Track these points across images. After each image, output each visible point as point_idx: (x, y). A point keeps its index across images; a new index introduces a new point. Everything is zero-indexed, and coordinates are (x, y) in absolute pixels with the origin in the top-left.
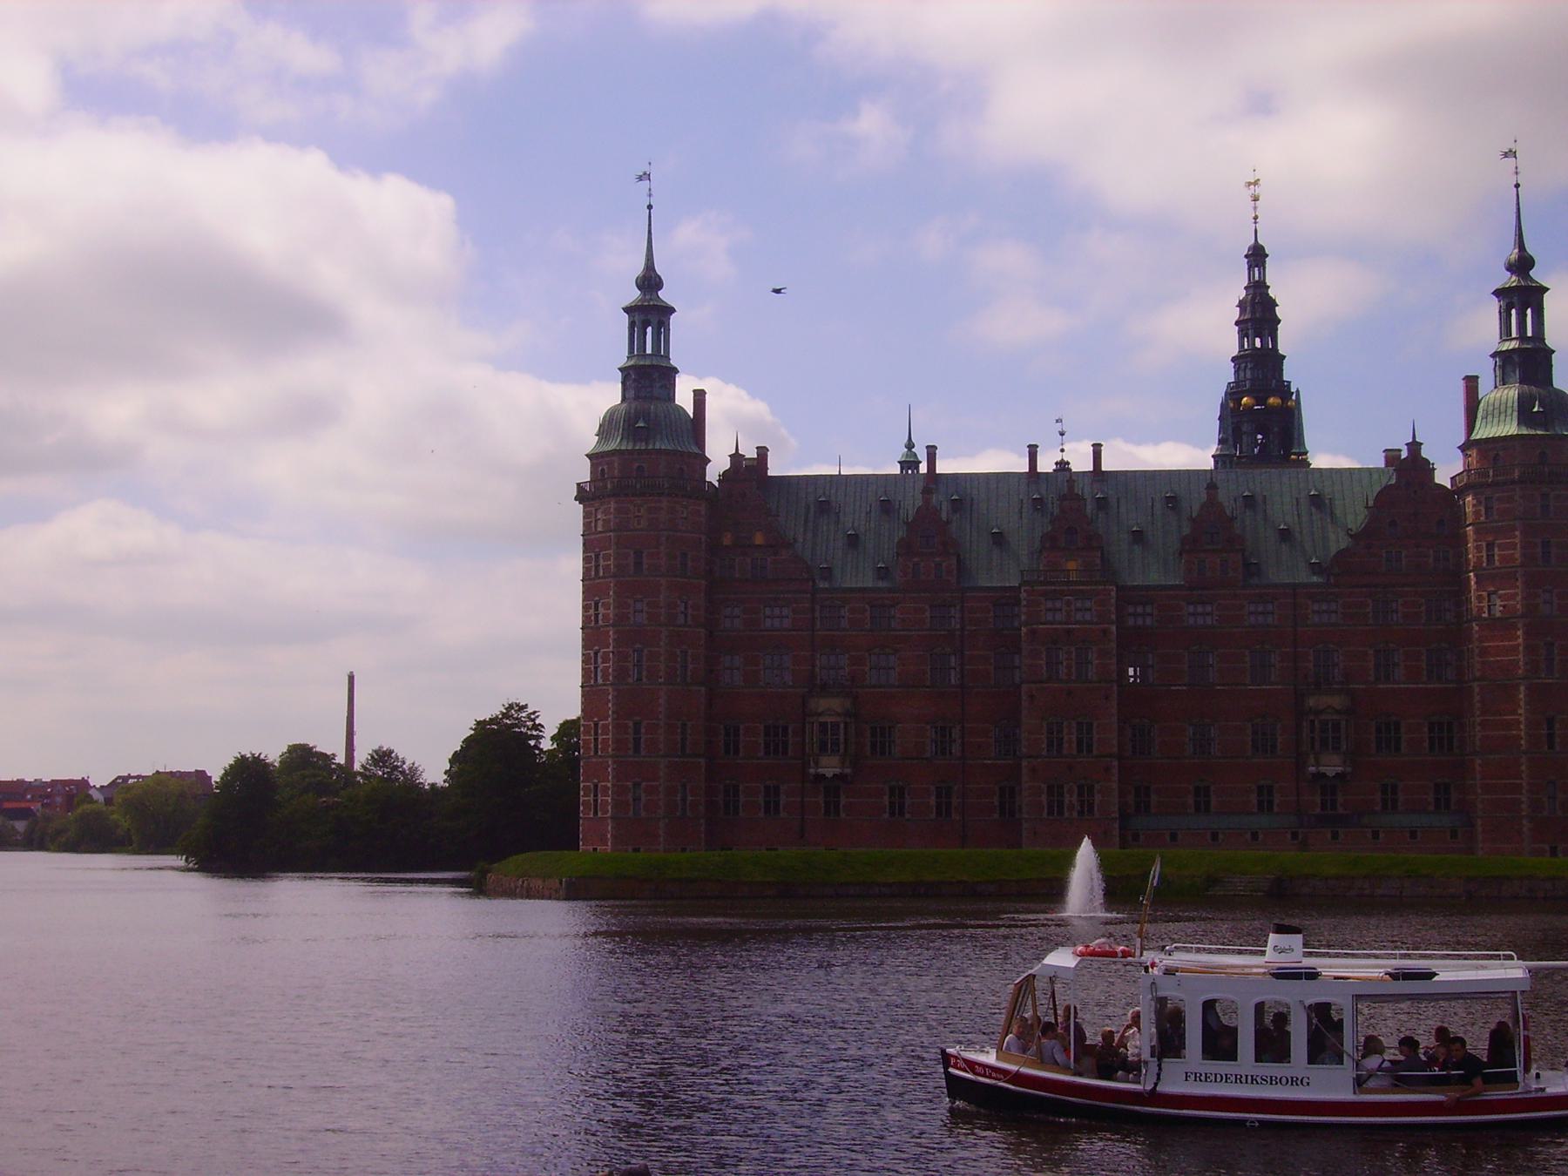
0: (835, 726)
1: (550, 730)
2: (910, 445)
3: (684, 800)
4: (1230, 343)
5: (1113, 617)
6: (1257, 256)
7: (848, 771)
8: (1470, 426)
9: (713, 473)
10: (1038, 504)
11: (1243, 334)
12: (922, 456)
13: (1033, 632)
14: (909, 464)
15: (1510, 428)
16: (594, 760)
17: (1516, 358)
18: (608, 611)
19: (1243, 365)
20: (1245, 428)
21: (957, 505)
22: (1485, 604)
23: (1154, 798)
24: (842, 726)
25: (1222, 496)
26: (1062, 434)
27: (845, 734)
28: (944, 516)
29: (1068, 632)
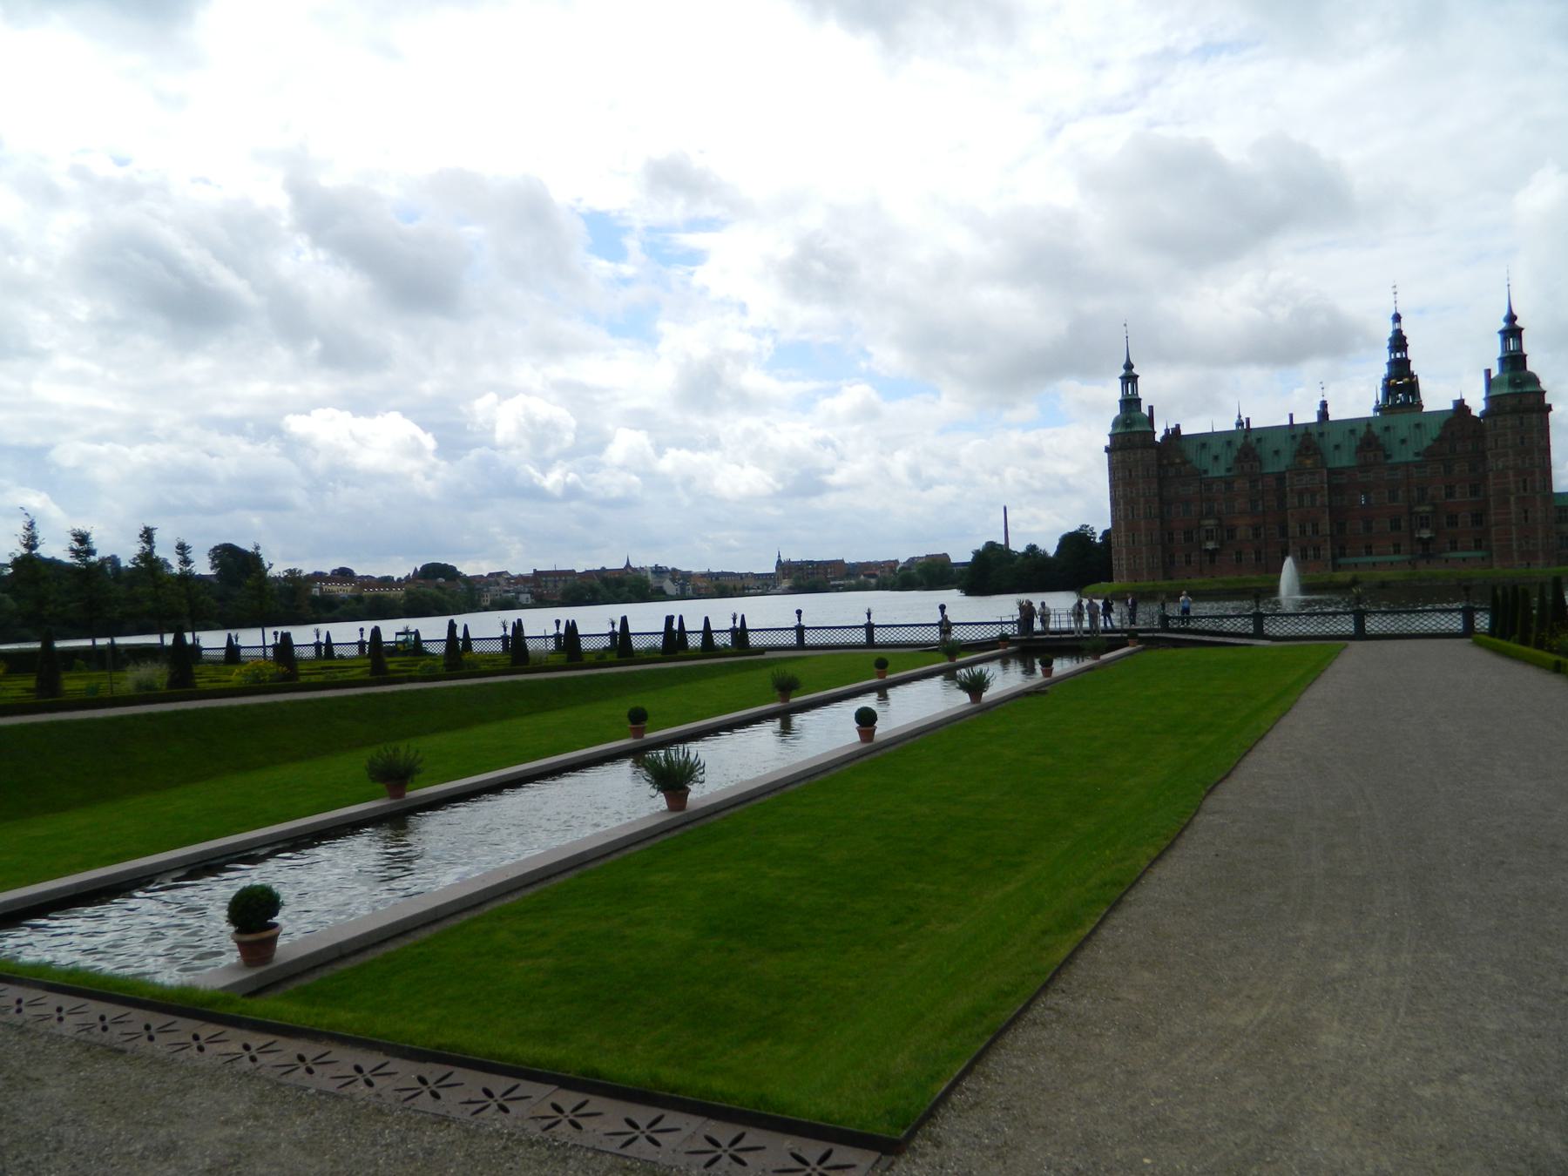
0: (1212, 531)
1: (1099, 534)
2: (1240, 416)
3: (1153, 562)
7: (1218, 547)
10: (1294, 437)
11: (1391, 352)
12: (1245, 421)
13: (1292, 490)
14: (1240, 424)
15: (1505, 390)
17: (1508, 360)
21: (1259, 440)
26: (1323, 388)
29: (1307, 489)
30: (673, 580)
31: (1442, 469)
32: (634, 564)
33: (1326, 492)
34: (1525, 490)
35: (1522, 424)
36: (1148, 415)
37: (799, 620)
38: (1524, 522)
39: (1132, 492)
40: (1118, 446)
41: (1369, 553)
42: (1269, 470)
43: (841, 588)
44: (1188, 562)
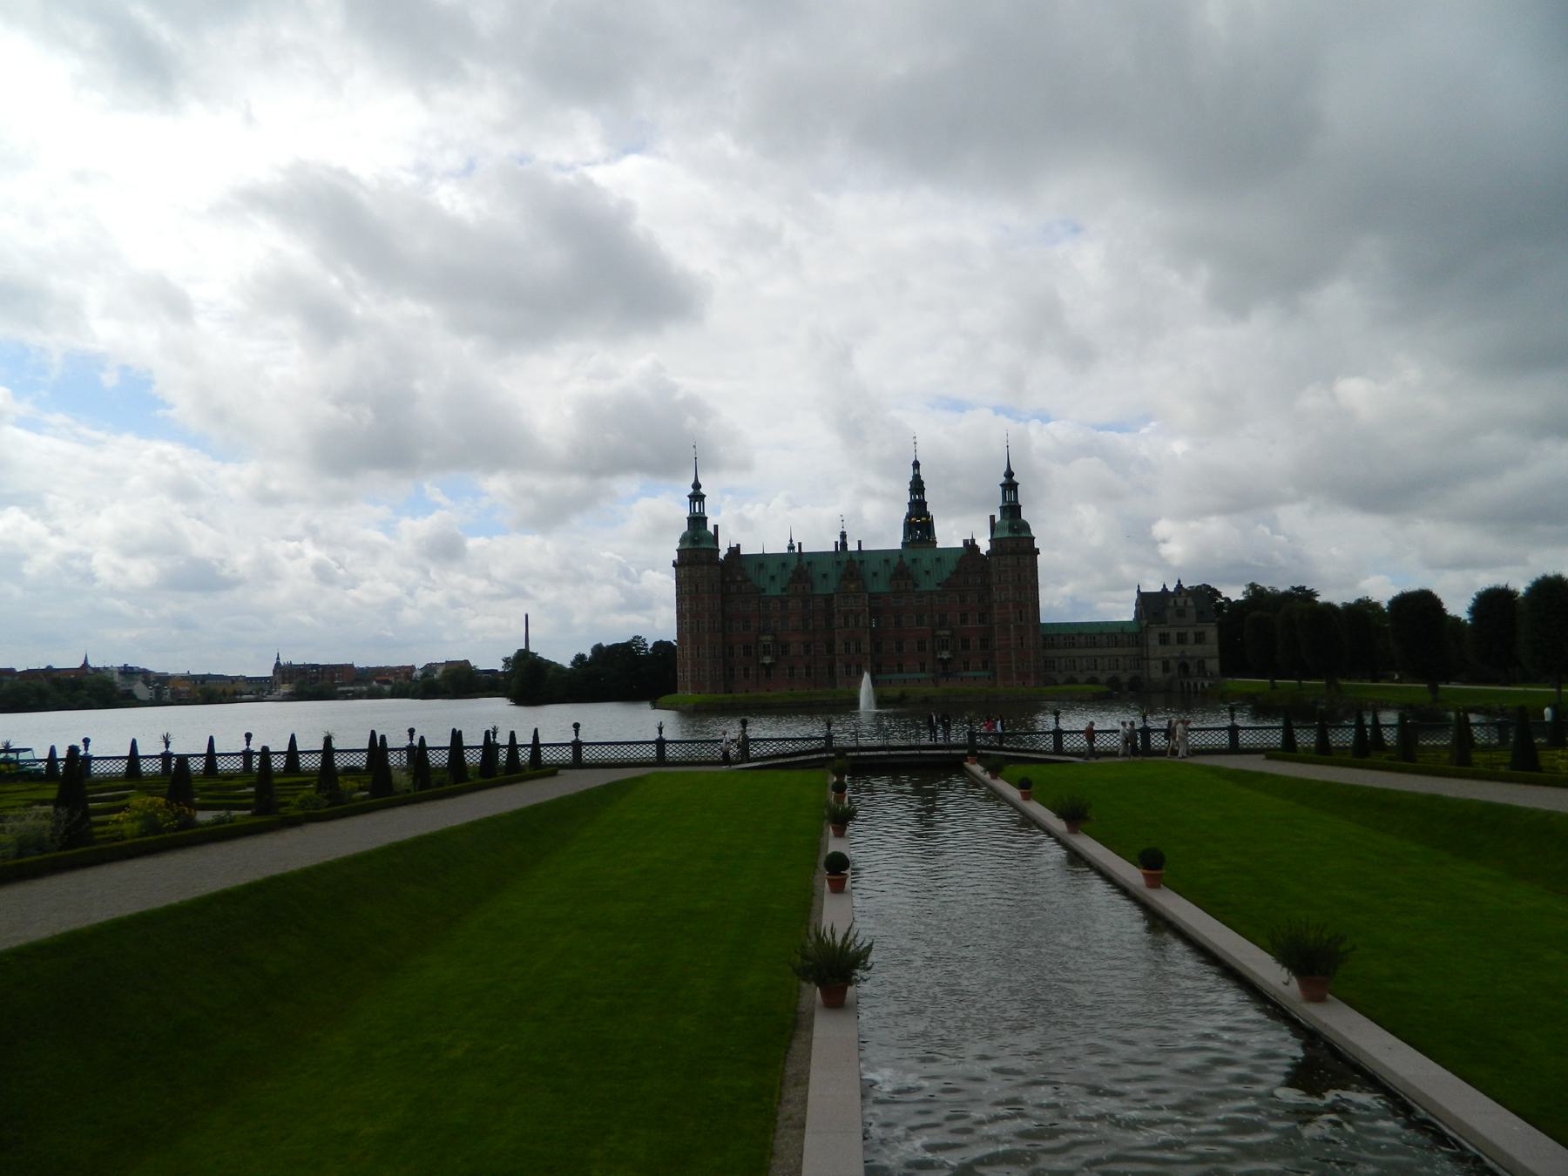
0: (769, 646)
1: (650, 646)
2: (791, 541)
4: (907, 497)
6: (916, 465)
7: (773, 661)
10: (839, 563)
14: (791, 547)
15: (1006, 534)
18: (686, 606)
21: (809, 564)
22: (998, 598)
23: (883, 668)
25: (905, 559)
28: (805, 568)
29: (852, 610)
30: (147, 682)
31: (958, 599)
32: (93, 663)
33: (867, 615)
34: (1021, 620)
35: (1018, 563)
37: (577, 734)
39: (697, 606)
40: (686, 561)
41: (900, 671)
42: (819, 591)
43: (350, 694)
44: (746, 675)
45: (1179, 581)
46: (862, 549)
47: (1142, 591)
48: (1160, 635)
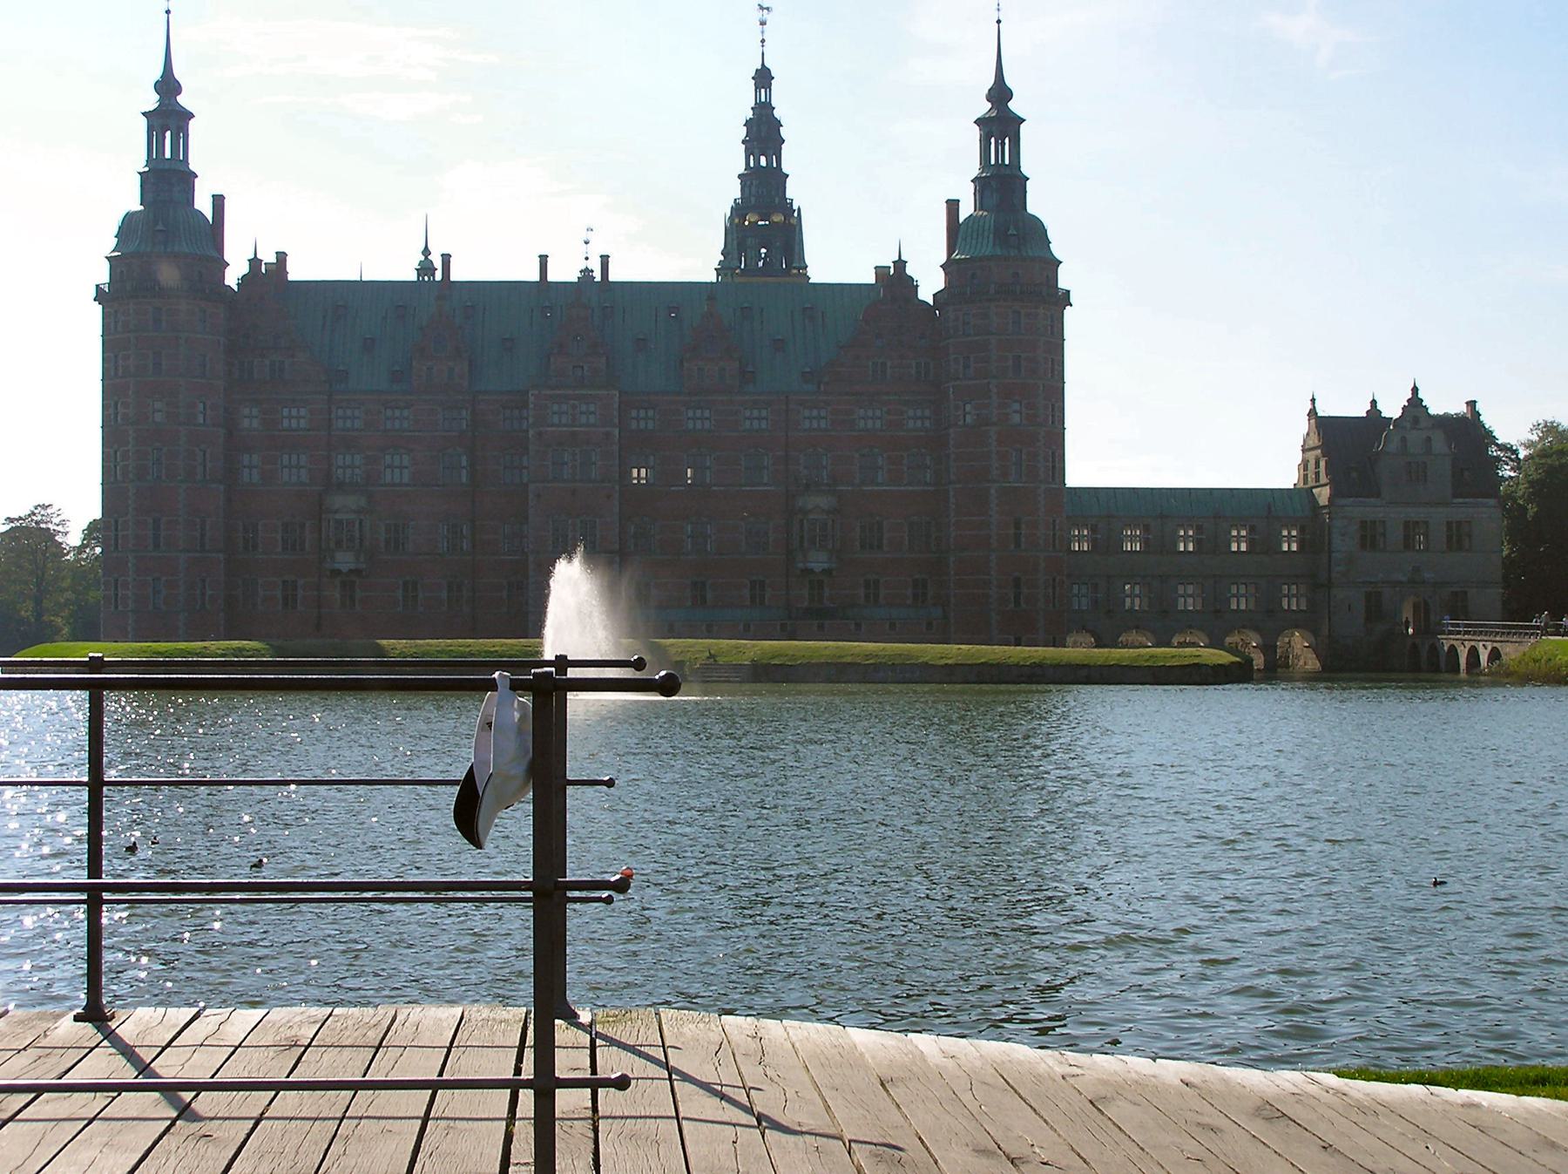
2: (426, 252)
4: (736, 161)
5: (616, 421)
6: (763, 78)
8: (950, 251)
9: (233, 276)
12: (438, 263)
13: (540, 434)
14: (426, 268)
15: (987, 250)
16: (115, 555)
17: (993, 183)
19: (748, 183)
20: (749, 241)
24: (357, 525)
26: (586, 243)
27: (360, 531)
36: (209, 216)
38: (1012, 547)
45: (1415, 390)
46: (612, 277)
47: (1320, 414)
48: (1363, 524)
